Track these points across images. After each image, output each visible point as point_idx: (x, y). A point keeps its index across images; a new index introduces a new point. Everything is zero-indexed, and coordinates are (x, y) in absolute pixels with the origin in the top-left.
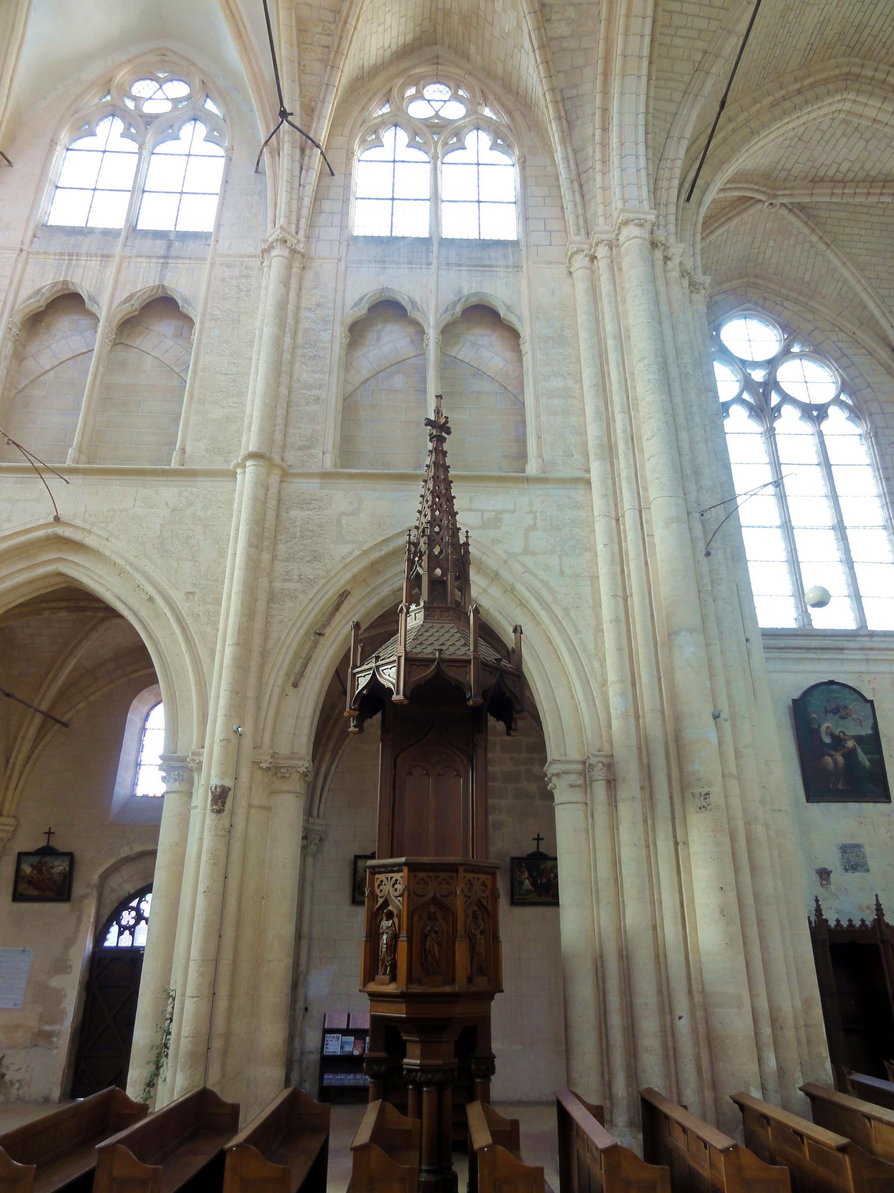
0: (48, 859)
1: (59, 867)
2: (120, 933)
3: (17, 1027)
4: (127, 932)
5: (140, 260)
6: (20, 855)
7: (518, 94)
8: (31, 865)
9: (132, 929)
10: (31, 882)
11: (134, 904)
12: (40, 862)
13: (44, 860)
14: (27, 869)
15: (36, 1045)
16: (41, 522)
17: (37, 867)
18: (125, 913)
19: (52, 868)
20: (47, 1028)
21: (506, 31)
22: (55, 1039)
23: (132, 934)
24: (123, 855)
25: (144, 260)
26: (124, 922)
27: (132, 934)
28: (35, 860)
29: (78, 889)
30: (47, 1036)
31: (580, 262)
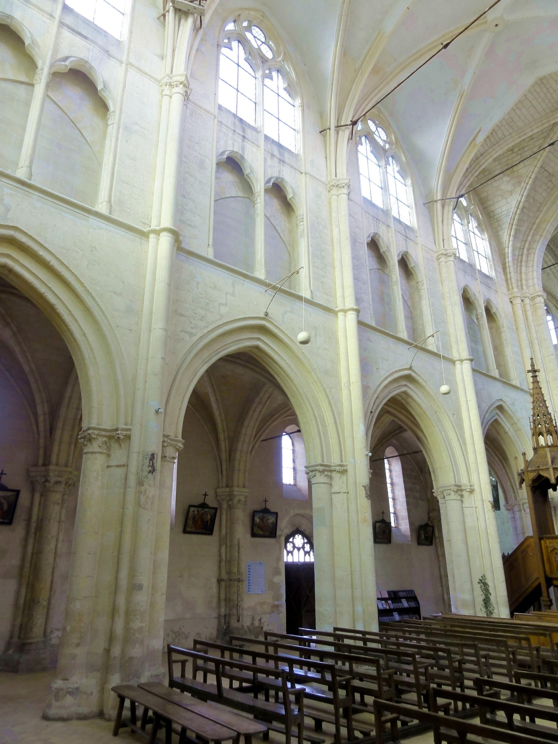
0: (266, 515)
1: (271, 519)
2: (288, 555)
3: (264, 603)
4: (290, 554)
5: (398, 234)
6: (254, 513)
7: (486, 208)
8: (259, 518)
9: (292, 552)
10: (260, 528)
11: (291, 540)
12: (263, 516)
13: (265, 515)
14: (257, 520)
15: (273, 612)
16: (406, 367)
17: (262, 519)
18: (288, 544)
19: (268, 520)
20: (276, 603)
21: (501, 188)
22: (280, 608)
23: (292, 555)
24: (292, 515)
25: (399, 234)
26: (288, 549)
27: (292, 555)
28: (261, 515)
29: (278, 533)
30: (277, 606)
31: (518, 301)
